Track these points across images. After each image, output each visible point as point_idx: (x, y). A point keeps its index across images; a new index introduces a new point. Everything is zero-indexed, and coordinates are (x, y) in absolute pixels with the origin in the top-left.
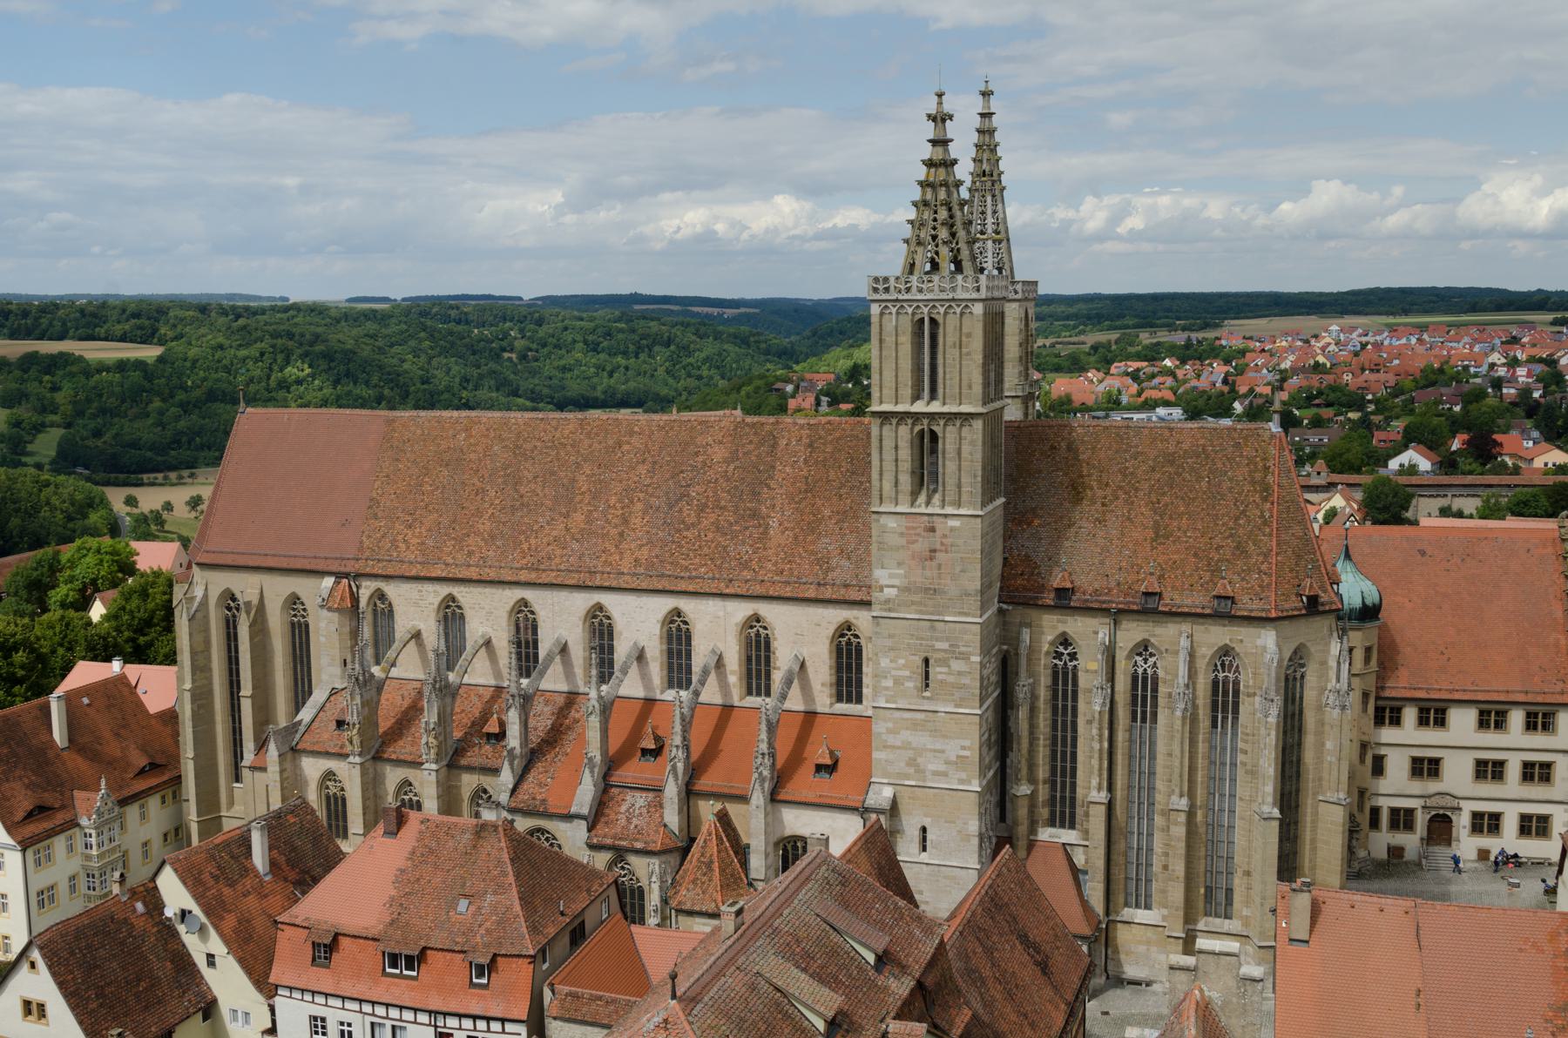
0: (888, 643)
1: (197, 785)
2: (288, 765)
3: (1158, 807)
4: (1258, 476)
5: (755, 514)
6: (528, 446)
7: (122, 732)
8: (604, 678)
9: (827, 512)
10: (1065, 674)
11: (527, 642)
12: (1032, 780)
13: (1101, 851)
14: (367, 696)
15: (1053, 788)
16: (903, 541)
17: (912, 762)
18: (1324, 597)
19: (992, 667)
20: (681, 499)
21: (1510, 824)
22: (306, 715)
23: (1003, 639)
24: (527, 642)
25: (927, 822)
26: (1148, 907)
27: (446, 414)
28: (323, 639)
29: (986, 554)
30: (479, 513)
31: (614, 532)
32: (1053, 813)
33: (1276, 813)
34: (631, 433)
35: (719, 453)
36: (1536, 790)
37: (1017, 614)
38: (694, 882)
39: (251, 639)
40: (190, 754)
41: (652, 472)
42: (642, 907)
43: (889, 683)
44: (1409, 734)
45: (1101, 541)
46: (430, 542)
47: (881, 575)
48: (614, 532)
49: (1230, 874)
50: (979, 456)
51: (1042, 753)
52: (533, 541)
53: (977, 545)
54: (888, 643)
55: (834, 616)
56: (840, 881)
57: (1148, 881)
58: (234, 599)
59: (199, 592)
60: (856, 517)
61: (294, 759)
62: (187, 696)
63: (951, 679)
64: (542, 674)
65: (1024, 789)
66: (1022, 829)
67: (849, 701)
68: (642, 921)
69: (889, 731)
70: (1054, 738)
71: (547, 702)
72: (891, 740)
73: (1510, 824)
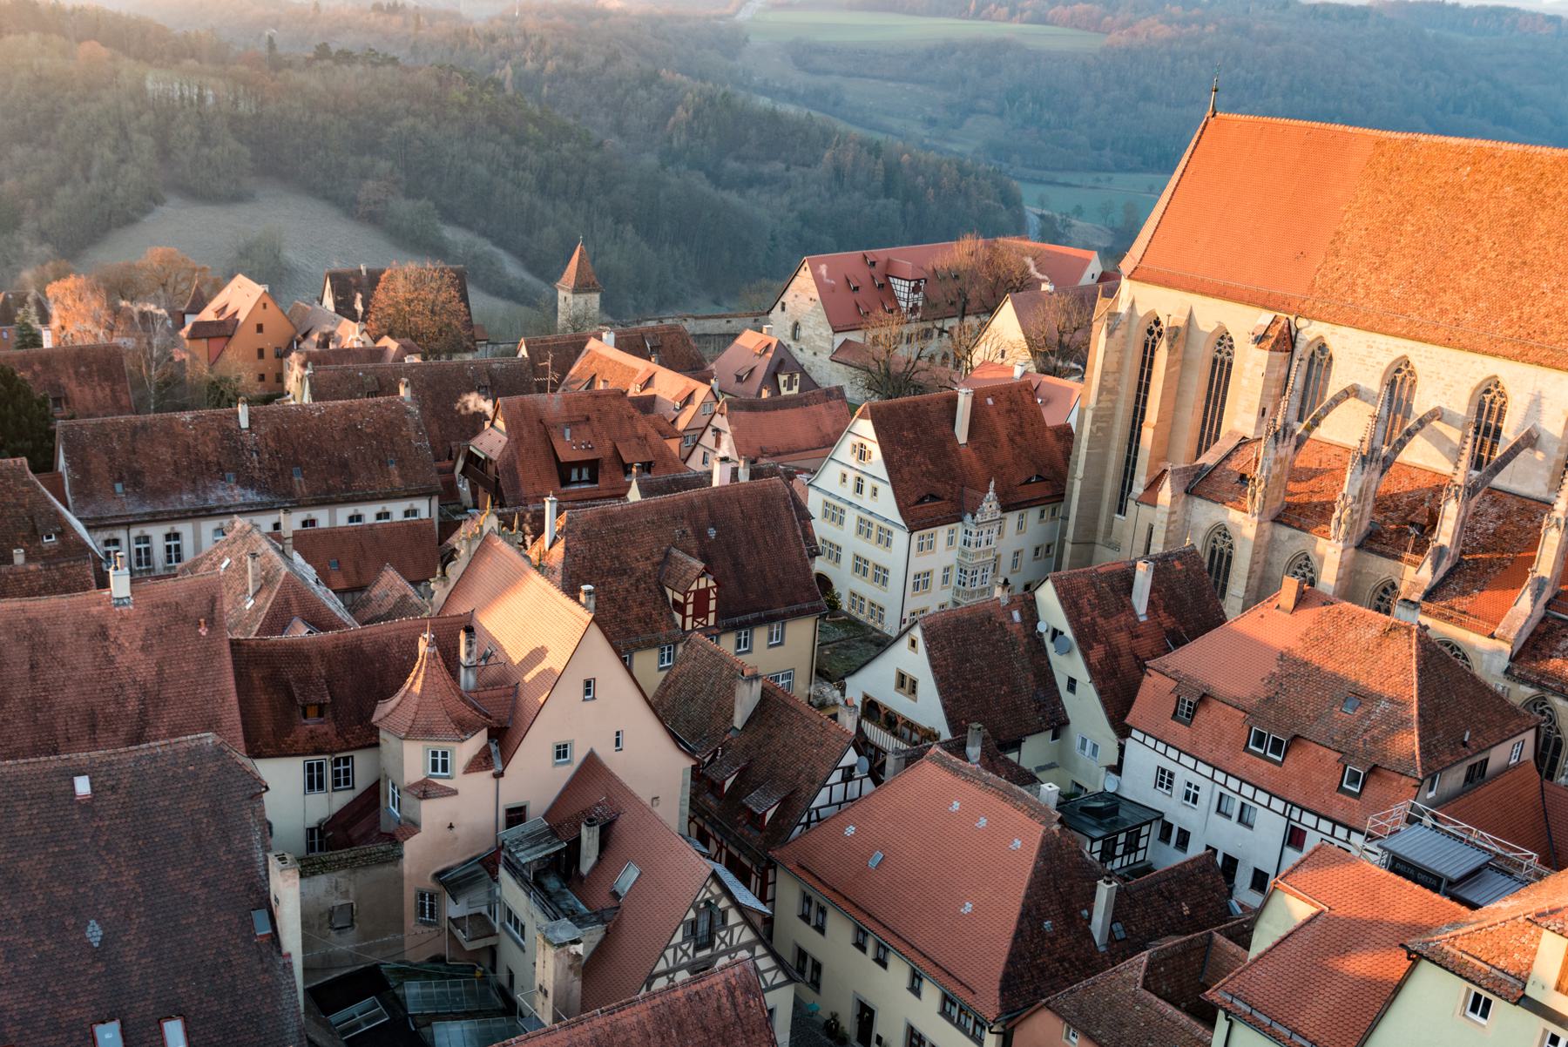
1: (1080, 508)
2: (1178, 508)
7: (1018, 438)
11: (1487, 428)
14: (1282, 453)
24: (1487, 428)
28: (1244, 382)
30: (1465, 266)
40: (1080, 473)
46: (1396, 292)
52: (1527, 309)
58: (1157, 323)
59: (1123, 308)
62: (1089, 415)
64: (1499, 467)
71: (1494, 503)
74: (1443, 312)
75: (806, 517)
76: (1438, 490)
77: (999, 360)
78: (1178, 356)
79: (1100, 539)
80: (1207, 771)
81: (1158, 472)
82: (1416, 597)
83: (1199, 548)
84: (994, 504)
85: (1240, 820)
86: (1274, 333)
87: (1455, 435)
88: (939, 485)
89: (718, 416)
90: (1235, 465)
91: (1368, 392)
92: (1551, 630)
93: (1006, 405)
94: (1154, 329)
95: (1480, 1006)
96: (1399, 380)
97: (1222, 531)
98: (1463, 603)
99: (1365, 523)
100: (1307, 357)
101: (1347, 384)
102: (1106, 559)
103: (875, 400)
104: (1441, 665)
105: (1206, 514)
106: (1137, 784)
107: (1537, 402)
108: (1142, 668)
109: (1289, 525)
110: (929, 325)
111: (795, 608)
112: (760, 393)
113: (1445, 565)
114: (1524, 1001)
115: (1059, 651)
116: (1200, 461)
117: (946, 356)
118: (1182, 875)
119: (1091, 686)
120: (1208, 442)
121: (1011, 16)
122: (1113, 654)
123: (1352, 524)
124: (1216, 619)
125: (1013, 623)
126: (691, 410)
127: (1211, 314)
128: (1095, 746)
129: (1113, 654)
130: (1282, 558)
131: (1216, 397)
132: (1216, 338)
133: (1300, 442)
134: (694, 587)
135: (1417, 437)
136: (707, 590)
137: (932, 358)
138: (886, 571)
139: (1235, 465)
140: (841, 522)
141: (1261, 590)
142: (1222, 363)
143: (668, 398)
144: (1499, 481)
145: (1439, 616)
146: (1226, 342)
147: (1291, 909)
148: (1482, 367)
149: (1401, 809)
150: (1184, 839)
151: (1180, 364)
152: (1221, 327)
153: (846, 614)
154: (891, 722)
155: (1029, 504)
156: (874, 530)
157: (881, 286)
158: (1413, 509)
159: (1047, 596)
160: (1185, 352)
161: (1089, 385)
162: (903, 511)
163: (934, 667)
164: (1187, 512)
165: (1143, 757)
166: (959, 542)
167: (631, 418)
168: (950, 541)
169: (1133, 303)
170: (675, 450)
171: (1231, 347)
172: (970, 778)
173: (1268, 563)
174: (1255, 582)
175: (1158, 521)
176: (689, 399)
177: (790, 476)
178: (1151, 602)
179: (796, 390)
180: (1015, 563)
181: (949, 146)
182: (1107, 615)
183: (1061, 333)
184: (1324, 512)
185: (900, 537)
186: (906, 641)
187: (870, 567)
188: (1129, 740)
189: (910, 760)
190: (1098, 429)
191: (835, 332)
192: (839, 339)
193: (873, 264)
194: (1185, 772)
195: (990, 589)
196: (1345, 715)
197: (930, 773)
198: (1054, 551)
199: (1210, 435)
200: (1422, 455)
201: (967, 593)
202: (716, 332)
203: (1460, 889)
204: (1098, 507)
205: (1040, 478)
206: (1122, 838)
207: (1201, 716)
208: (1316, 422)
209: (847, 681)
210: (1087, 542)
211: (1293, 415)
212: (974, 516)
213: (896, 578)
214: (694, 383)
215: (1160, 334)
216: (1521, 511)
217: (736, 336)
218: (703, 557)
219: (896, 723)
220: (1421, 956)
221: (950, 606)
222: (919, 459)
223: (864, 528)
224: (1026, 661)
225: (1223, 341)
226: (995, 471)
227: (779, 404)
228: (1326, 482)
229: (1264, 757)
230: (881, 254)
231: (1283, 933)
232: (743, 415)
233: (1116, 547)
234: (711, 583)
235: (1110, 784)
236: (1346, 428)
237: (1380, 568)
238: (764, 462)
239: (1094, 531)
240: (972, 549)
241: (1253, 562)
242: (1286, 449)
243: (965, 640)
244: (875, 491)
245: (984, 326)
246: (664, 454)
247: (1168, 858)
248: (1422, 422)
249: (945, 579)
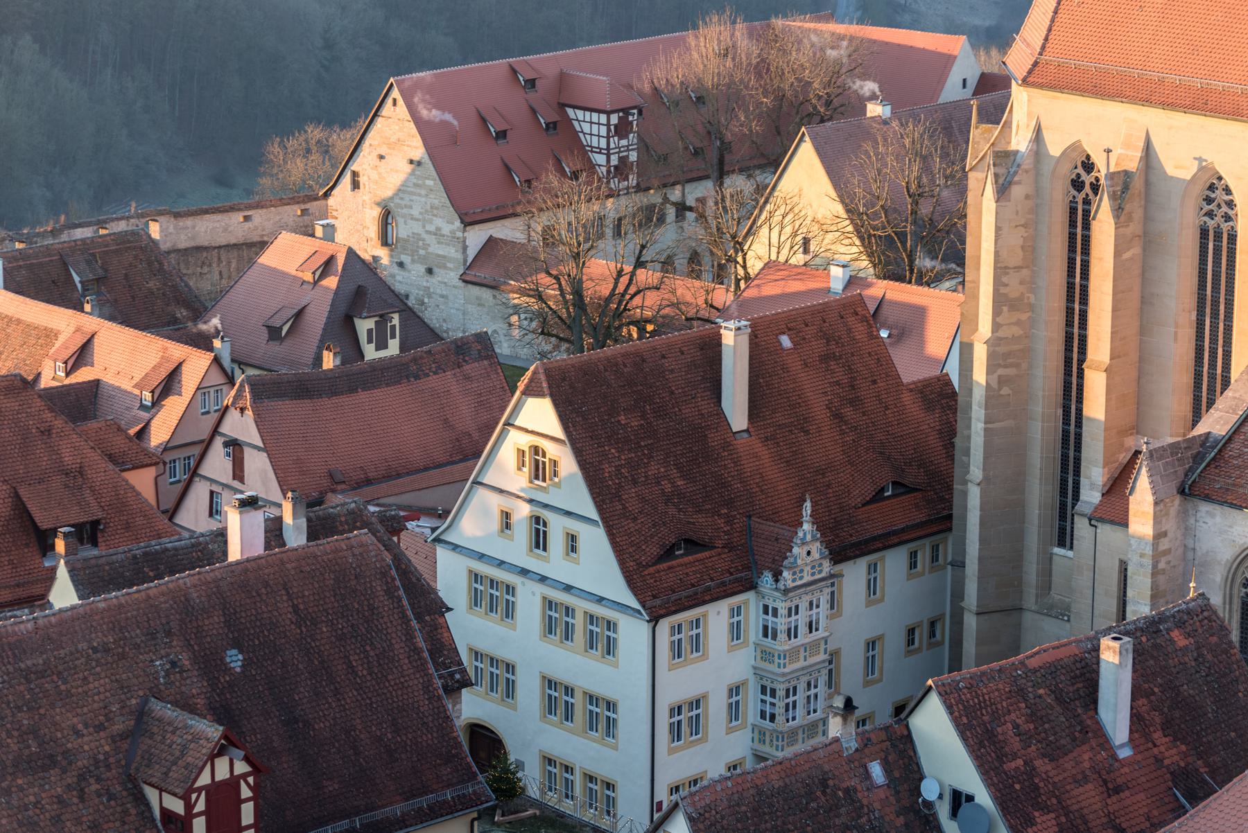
7: (848, 412)
39: (1117, 254)
58: (1088, 166)
59: (1020, 142)
75: (431, 608)
77: (799, 259)
81: (1124, 457)
84: (816, 548)
88: (701, 519)
89: (233, 415)
94: (1082, 179)
103: (562, 356)
110: (654, 197)
111: (424, 801)
112: (318, 360)
116: (1201, 429)
117: (694, 258)
120: (1212, 390)
125: (872, 787)
126: (174, 407)
131: (1215, 303)
132: (1199, 189)
134: (204, 779)
136: (233, 783)
140: (509, 611)
142: (1218, 236)
143: (127, 385)
146: (1220, 195)
151: (1143, 244)
153: (534, 803)
156: (579, 622)
157: (552, 126)
159: (933, 724)
160: (1147, 218)
161: (975, 297)
162: (633, 579)
164: (1188, 531)
166: (753, 631)
167: (47, 432)
168: (736, 631)
169: (1038, 131)
170: (148, 493)
171: (1231, 204)
176: (169, 384)
177: (394, 526)
179: (394, 348)
182: (1054, 753)
185: (633, 633)
190: (1002, 381)
191: (468, 222)
192: (476, 237)
193: (531, 83)
195: (825, 721)
199: (1212, 377)
201: (779, 735)
202: (222, 240)
204: (1018, 536)
212: (777, 576)
214: (178, 351)
215: (1095, 188)
217: (262, 245)
218: (220, 713)
221: (749, 765)
222: (654, 469)
223: (556, 622)
227: (358, 378)
230: (545, 63)
232: (286, 408)
234: (241, 767)
238: (338, 502)
239: (1015, 584)
244: (572, 542)
245: (763, 193)
246: (124, 501)
249: (734, 711)
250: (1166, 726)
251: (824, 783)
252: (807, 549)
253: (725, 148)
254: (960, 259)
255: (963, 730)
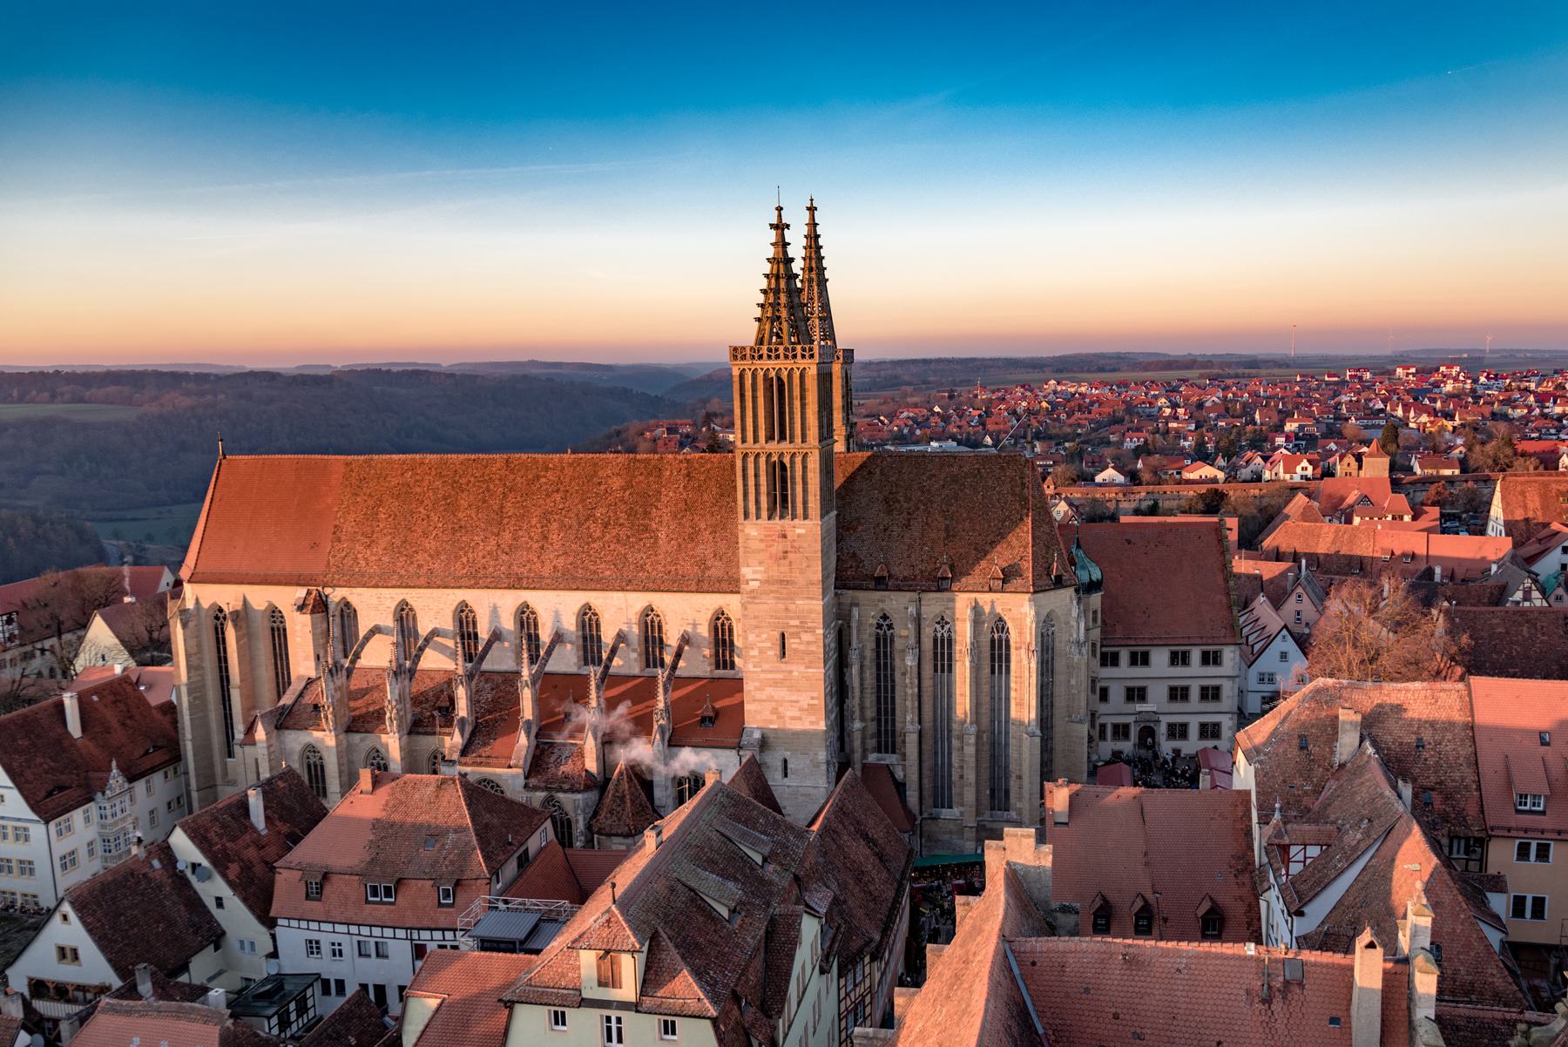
0: (753, 622)
2: (273, 741)
3: (954, 733)
4: (1017, 490)
5: (646, 529)
6: (463, 481)
7: (128, 722)
8: (533, 659)
9: (703, 526)
10: (885, 640)
12: (863, 719)
13: (915, 768)
14: (339, 683)
15: (879, 721)
16: (763, 546)
17: (775, 711)
18: (1066, 576)
19: (832, 636)
20: (587, 520)
21: (1194, 731)
22: (287, 700)
23: (838, 616)
25: (788, 754)
26: (950, 807)
27: (395, 457)
29: (825, 553)
30: (425, 534)
31: (536, 546)
32: (879, 743)
33: (1038, 732)
34: (547, 469)
35: (617, 483)
36: (1211, 706)
37: (849, 595)
38: (611, 812)
40: (188, 735)
41: (564, 499)
42: (570, 834)
43: (755, 653)
44: (1125, 671)
45: (907, 541)
46: (386, 559)
47: (746, 572)
48: (536, 546)
49: (1007, 778)
50: (818, 480)
51: (870, 700)
53: (818, 546)
54: (753, 622)
55: (706, 604)
56: (726, 800)
57: (950, 789)
58: (221, 610)
59: (190, 605)
60: (724, 529)
61: (278, 737)
62: (184, 690)
63: (802, 647)
64: (482, 658)
65: (857, 725)
66: (857, 756)
67: (725, 668)
68: (571, 845)
69: (757, 689)
70: (879, 687)
71: (487, 681)
72: (758, 695)
73: (1194, 731)
74: (420, 566)
76: (449, 682)
77: (101, 663)
78: (244, 631)
79: (219, 781)
80: (343, 928)
82: (455, 756)
83: (296, 766)
84: (121, 779)
85: (378, 955)
86: (311, 601)
87: (450, 643)
88: (63, 777)
90: (308, 699)
91: (387, 628)
92: (543, 752)
93: (111, 698)
94: (218, 614)
95: (559, 1019)
96: (404, 616)
97: (311, 749)
98: (486, 751)
99: (409, 716)
100: (338, 613)
101: (371, 626)
102: (227, 794)
104: (481, 795)
105: (296, 740)
106: (295, 960)
107: (495, 610)
108: (272, 869)
109: (358, 732)
110: (28, 648)
113: (468, 729)
114: (585, 1003)
115: (202, 879)
117: (52, 670)
118: (343, 1016)
119: (236, 899)
121: (53, 398)
122: (247, 867)
123: (400, 719)
124: (322, 813)
127: (259, 597)
128: (252, 944)
129: (247, 867)
130: (360, 756)
132: (269, 613)
133: (349, 672)
135: (427, 650)
137: (40, 674)
138: (30, 863)
139: (308, 699)
141: (350, 781)
144: (486, 666)
145: (474, 764)
147: (423, 1007)
148: (455, 596)
149: (478, 904)
150: (341, 985)
151: (246, 638)
152: (271, 604)
154: (61, 992)
155: (153, 770)
156: (10, 831)
158: (438, 698)
162: (34, 807)
163: (90, 931)
165: (292, 936)
168: (87, 820)
172: (143, 1014)
173: (350, 762)
174: (345, 778)
175: (260, 753)
178: (267, 818)
180: (152, 820)
181: (20, 503)
182: (234, 839)
183: (150, 632)
184: (380, 715)
185: (38, 830)
186: (57, 918)
187: (14, 864)
188: (278, 929)
189: (83, 1019)
194: (326, 935)
195: (129, 851)
196: (428, 853)
197: (103, 1022)
198: (184, 800)
200: (434, 661)
201: (113, 857)
203: (527, 945)
204: (211, 758)
205: (156, 748)
206: (292, 1006)
207: (328, 889)
208: (357, 656)
209: (8, 972)
210: (209, 786)
211: (340, 655)
213: (42, 867)
216: (505, 681)
219: (67, 991)
220: (513, 1002)
222: (38, 760)
224: (175, 898)
225: (274, 613)
226: (116, 752)
228: (376, 695)
229: (381, 903)
231: (421, 1028)
233: (233, 783)
235: (271, 968)
236: (378, 655)
237: (427, 743)
239: (213, 776)
240: (110, 820)
241: (340, 765)
242: (341, 679)
243: (113, 899)
245: (81, 639)
247: (335, 1003)
248: (427, 640)
249: (91, 852)
250: (281, 818)
251: (132, 874)
252: (116, 779)
253: (60, 623)
254: (170, 652)
255: (192, 839)
